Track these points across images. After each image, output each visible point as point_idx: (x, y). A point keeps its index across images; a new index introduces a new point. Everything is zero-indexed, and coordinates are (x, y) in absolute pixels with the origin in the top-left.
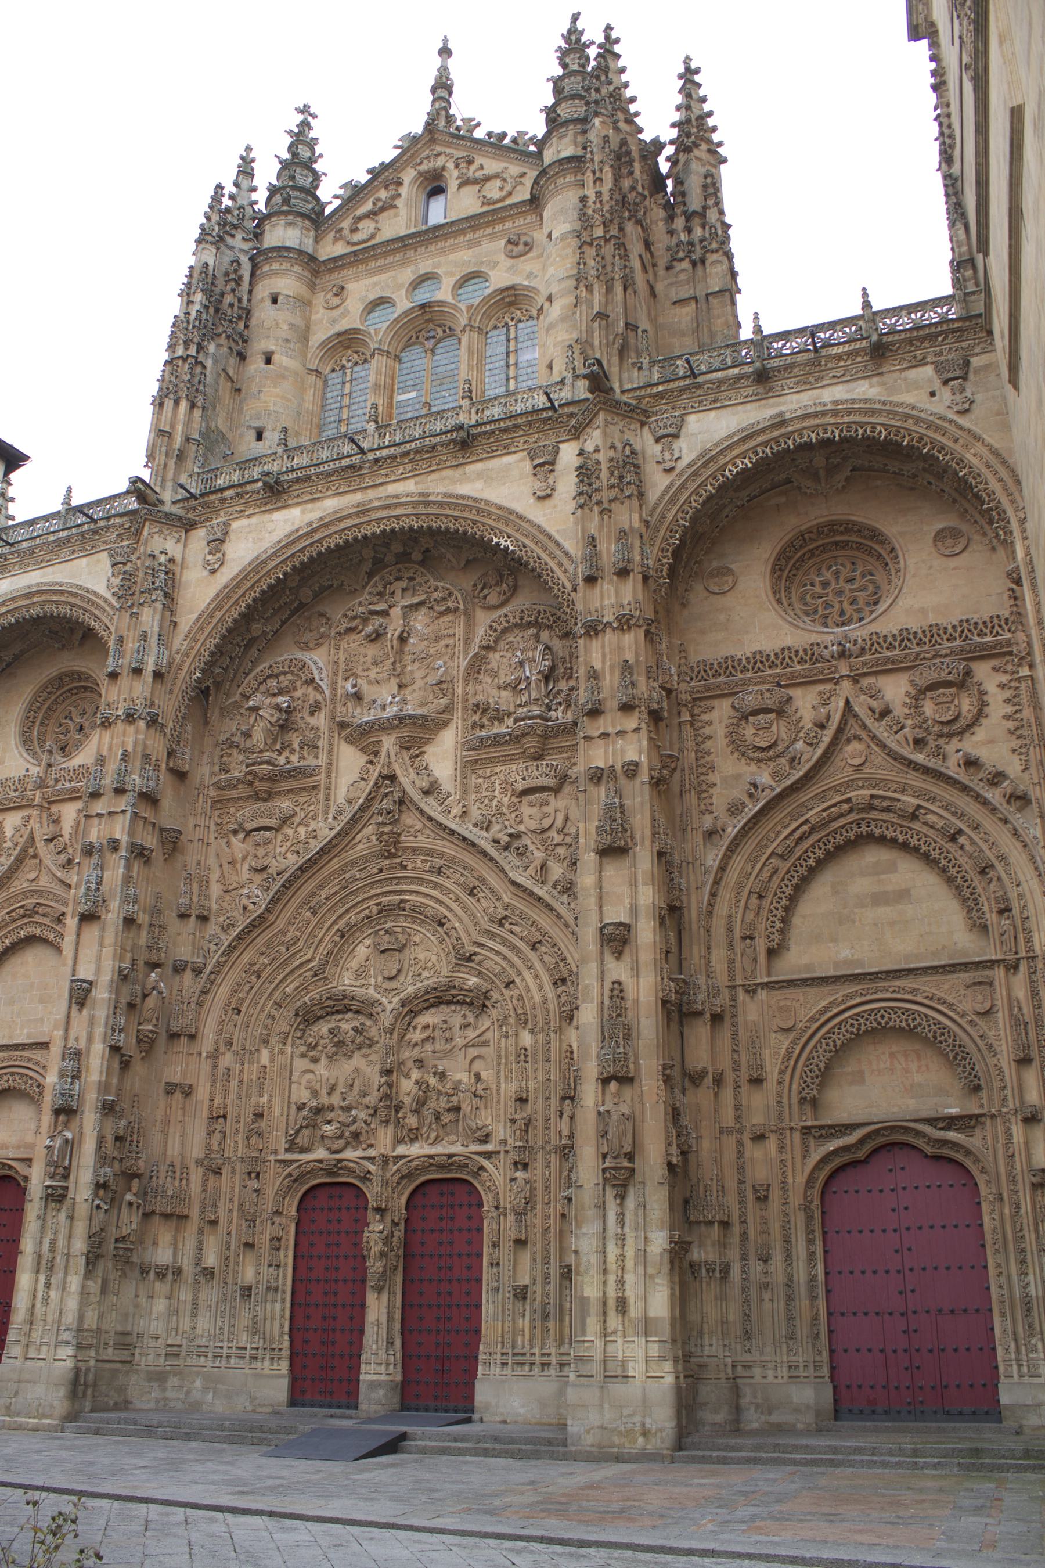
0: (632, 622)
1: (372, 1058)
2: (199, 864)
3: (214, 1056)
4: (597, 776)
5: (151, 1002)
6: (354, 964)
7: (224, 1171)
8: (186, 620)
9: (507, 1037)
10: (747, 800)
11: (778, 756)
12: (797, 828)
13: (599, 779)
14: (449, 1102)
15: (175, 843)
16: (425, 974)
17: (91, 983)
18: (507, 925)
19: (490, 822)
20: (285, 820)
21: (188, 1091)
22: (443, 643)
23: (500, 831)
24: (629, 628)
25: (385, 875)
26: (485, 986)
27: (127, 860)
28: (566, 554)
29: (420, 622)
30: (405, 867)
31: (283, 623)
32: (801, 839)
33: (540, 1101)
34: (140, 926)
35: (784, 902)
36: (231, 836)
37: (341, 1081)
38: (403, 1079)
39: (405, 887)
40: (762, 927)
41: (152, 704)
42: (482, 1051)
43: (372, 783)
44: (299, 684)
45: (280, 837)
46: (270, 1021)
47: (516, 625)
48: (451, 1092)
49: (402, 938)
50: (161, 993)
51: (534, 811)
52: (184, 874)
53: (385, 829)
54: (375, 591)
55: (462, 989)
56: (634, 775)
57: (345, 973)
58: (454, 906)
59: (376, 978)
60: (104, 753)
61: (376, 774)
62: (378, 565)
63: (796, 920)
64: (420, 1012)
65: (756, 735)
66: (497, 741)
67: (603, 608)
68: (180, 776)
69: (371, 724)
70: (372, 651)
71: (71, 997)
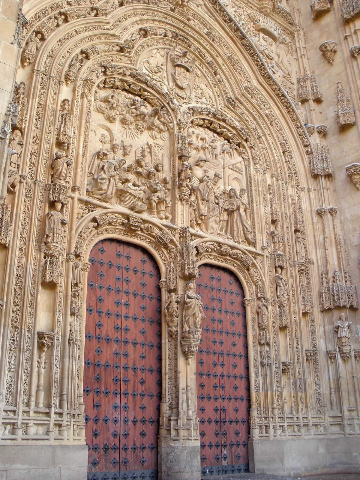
1: (157, 141)
6: (153, 62)
7: (17, 189)
16: (204, 100)
42: (240, 176)
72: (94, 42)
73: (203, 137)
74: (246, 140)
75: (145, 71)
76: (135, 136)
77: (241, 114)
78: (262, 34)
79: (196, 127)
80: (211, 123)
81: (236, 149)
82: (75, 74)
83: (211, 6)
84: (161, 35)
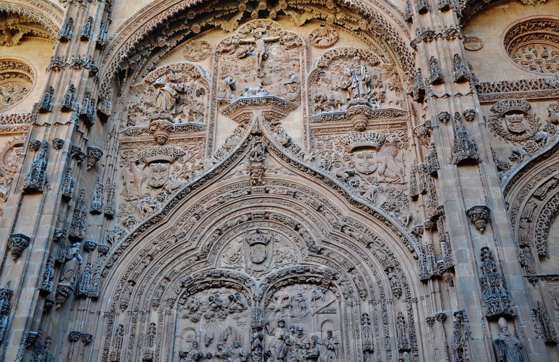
0: (457, 34)
1: (240, 320)
2: (109, 180)
3: (111, 315)
4: (446, 119)
5: (71, 264)
6: (230, 253)
8: (118, 22)
9: (352, 306)
10: (511, 163)
11: (528, 139)
12: (547, 182)
13: (448, 120)
14: (308, 353)
15: (97, 160)
16: (285, 261)
17: (28, 240)
18: (347, 231)
19: (331, 166)
20: (178, 157)
21: (88, 340)
22: (291, 63)
23: (343, 170)
24: (454, 39)
25: (253, 195)
26: (333, 271)
27: (69, 155)
28: (392, 6)
29: (275, 50)
30: (267, 192)
31: (178, 43)
32: (550, 188)
33: (383, 352)
34: (69, 208)
35: (544, 226)
36: (134, 165)
37: (217, 336)
38: (267, 336)
39: (268, 204)
40: (535, 239)
41: (93, 63)
42: (331, 316)
43: (246, 137)
44: (189, 78)
45: (172, 167)
46: (161, 291)
47: (341, 57)
48: (308, 346)
49: (268, 237)
50: (79, 260)
51: (362, 161)
52: (98, 186)
53: (256, 165)
54: (243, 31)
55: (314, 273)
56: (473, 120)
57: (222, 259)
58: (306, 218)
59: (246, 262)
60: (54, 86)
61: (249, 132)
62: (247, 17)
63: (550, 240)
64: (280, 288)
65: (513, 126)
66: (335, 117)
67: (434, 27)
68: (104, 118)
69: (246, 101)
70: (242, 63)
71: (8, 249)
72: (176, 263)
73: (285, 297)
74: (335, 279)
75: (223, 265)
76: (218, 324)
77: (328, 255)
78: (356, 153)
79: (283, 289)
80: (296, 278)
81: (329, 289)
82: (157, 300)
83: (288, 164)
84: (237, 224)
